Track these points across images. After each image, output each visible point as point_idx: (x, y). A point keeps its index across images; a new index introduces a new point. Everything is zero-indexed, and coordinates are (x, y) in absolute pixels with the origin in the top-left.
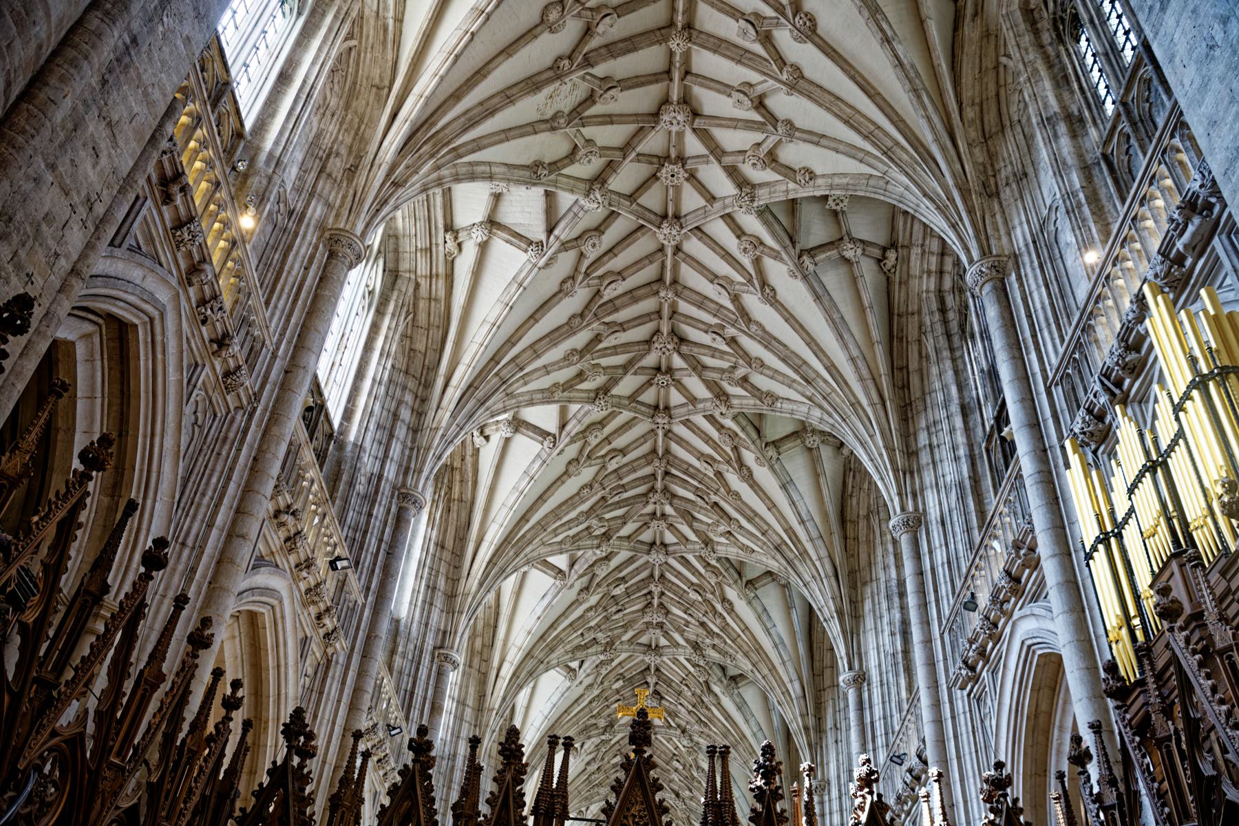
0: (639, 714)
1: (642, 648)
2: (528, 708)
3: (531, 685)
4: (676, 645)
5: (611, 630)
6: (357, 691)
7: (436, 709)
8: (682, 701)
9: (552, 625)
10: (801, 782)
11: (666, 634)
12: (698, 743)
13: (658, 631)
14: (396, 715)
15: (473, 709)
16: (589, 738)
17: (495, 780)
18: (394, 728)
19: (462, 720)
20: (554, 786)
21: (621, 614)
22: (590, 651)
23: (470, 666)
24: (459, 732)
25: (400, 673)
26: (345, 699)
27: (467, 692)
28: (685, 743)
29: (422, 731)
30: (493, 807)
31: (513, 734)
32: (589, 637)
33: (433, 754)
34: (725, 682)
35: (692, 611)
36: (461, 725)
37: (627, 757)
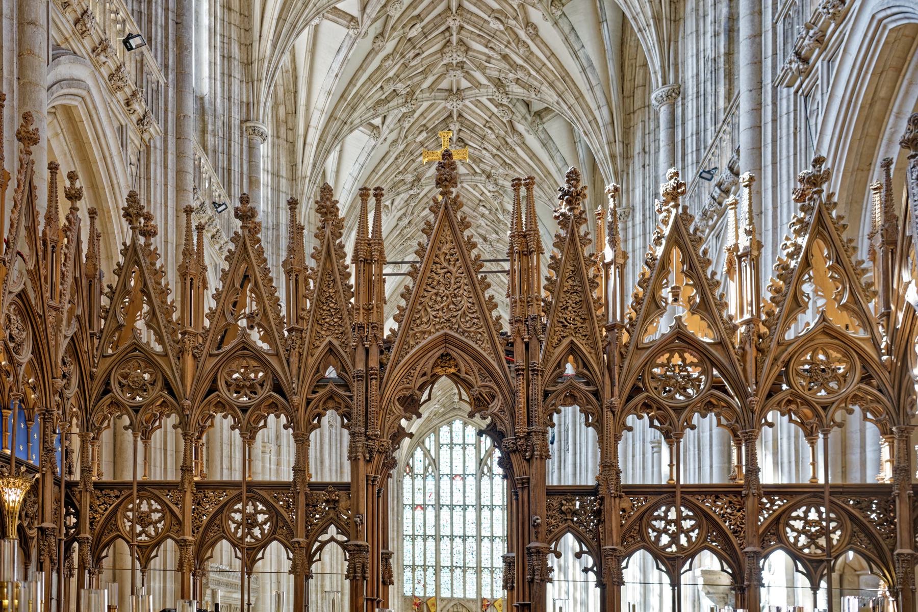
0: (443, 155)
1: (443, 94)
2: (338, 172)
3: (338, 148)
4: (479, 85)
5: (411, 78)
6: (180, 173)
7: (253, 182)
8: (486, 145)
9: (350, 82)
10: (604, 203)
11: (467, 75)
12: (503, 186)
13: (459, 72)
14: (219, 193)
15: (287, 179)
16: (398, 194)
17: (316, 236)
18: (220, 205)
19: (279, 191)
20: (370, 236)
21: (419, 59)
22: (391, 104)
23: (278, 137)
24: (278, 203)
25: (215, 151)
26: (171, 183)
27: (279, 164)
28: (491, 188)
29: (244, 199)
30: (317, 260)
31: (326, 191)
32: (389, 89)
33: (257, 220)
34: (529, 118)
35: (494, 43)
36: (278, 196)
37: (435, 200)
